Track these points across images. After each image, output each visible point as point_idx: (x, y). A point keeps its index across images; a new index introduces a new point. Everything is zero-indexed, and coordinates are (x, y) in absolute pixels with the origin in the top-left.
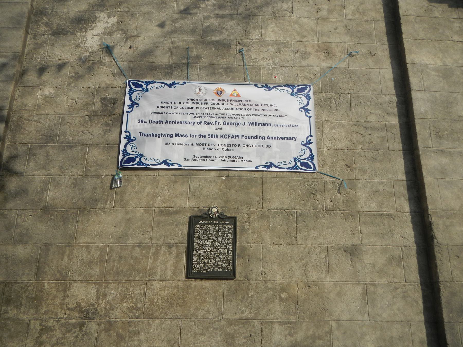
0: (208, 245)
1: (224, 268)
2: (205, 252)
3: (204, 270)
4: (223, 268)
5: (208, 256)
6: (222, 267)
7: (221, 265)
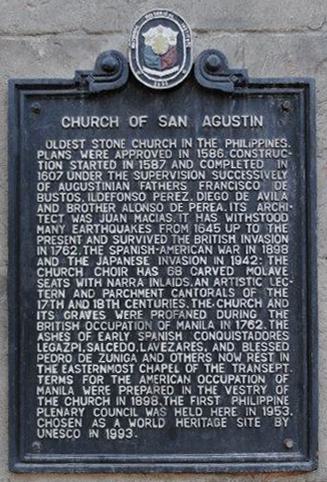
0: (132, 271)
1: (242, 410)
2: (110, 314)
3: (110, 422)
4: (232, 412)
5: (134, 336)
6: (226, 401)
7: (221, 389)
